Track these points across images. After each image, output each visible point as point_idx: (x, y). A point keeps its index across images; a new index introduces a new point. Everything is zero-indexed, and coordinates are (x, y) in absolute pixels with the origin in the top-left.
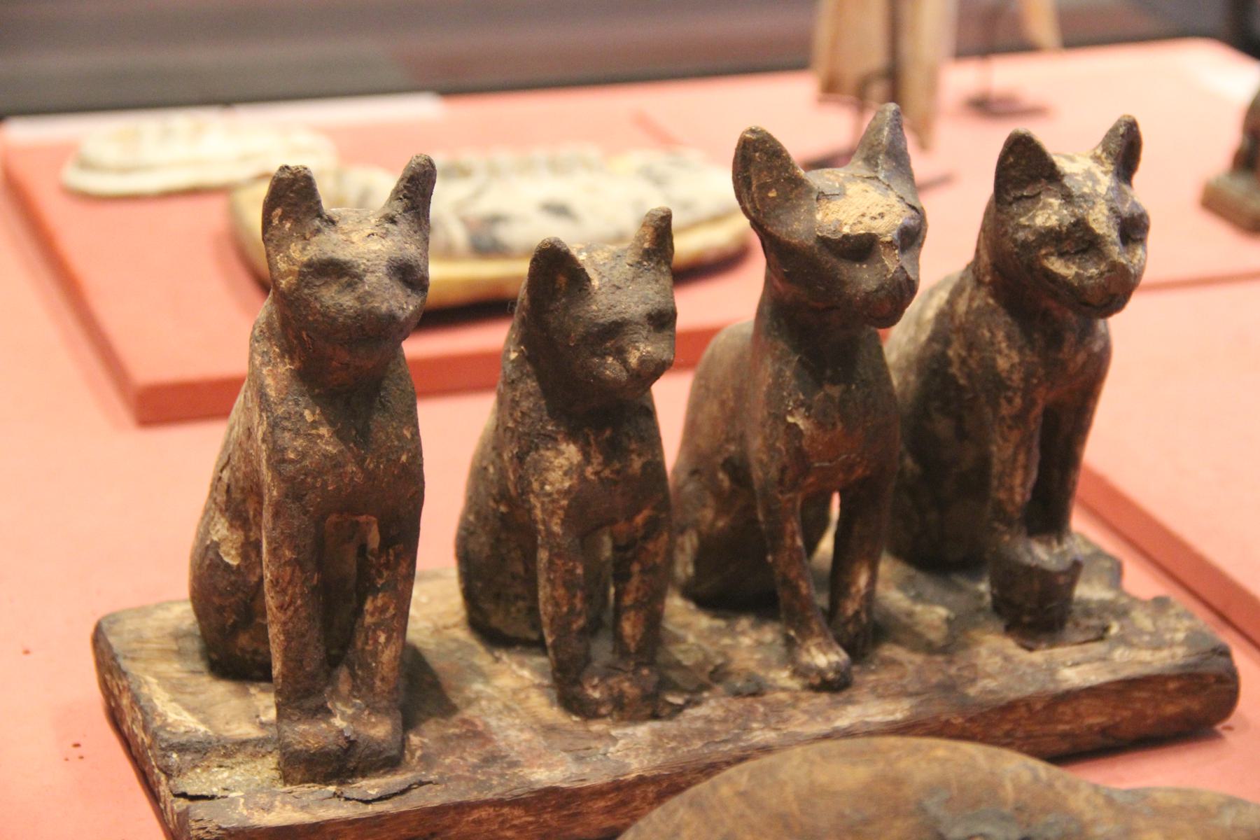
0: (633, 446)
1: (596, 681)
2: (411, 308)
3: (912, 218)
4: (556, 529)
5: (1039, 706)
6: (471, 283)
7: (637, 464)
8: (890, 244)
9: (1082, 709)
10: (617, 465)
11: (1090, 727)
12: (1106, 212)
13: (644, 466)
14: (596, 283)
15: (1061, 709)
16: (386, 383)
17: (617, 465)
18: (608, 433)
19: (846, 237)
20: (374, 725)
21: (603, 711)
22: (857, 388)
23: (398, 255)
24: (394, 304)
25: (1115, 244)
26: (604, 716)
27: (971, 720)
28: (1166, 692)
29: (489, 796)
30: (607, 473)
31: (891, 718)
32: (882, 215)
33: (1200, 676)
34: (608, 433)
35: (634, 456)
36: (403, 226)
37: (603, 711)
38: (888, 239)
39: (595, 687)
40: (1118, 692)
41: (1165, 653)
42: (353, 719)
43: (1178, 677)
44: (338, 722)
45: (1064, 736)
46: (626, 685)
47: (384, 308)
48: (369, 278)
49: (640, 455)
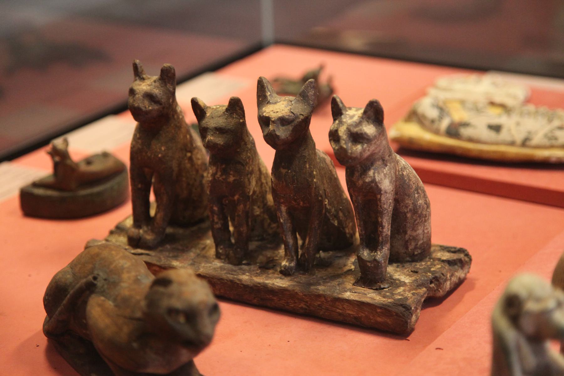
0: (232, 173)
1: (222, 247)
2: (150, 108)
3: (289, 116)
4: (208, 192)
5: (329, 300)
6: (441, 145)
7: (231, 179)
8: (273, 122)
9: (345, 306)
10: (224, 177)
11: (349, 314)
12: (345, 129)
13: (234, 180)
14: (208, 115)
15: (337, 303)
16: (161, 132)
17: (224, 177)
18: (224, 166)
19: (263, 116)
20: (149, 235)
21: (222, 257)
22: (291, 172)
23: (149, 91)
24: (141, 105)
25: (344, 140)
26: (222, 259)
27: (305, 295)
28: (377, 312)
29: (158, 264)
30: (221, 179)
31: (281, 285)
32: (277, 112)
33: (389, 311)
34: (224, 166)
35: (231, 176)
36: (157, 84)
37: (222, 257)
38: (273, 120)
39: (221, 249)
40: (358, 305)
41: (384, 299)
42: (145, 232)
43: (381, 308)
44: (141, 231)
45: (340, 314)
46: (231, 252)
47: (136, 105)
48: (137, 96)
49: (234, 176)
